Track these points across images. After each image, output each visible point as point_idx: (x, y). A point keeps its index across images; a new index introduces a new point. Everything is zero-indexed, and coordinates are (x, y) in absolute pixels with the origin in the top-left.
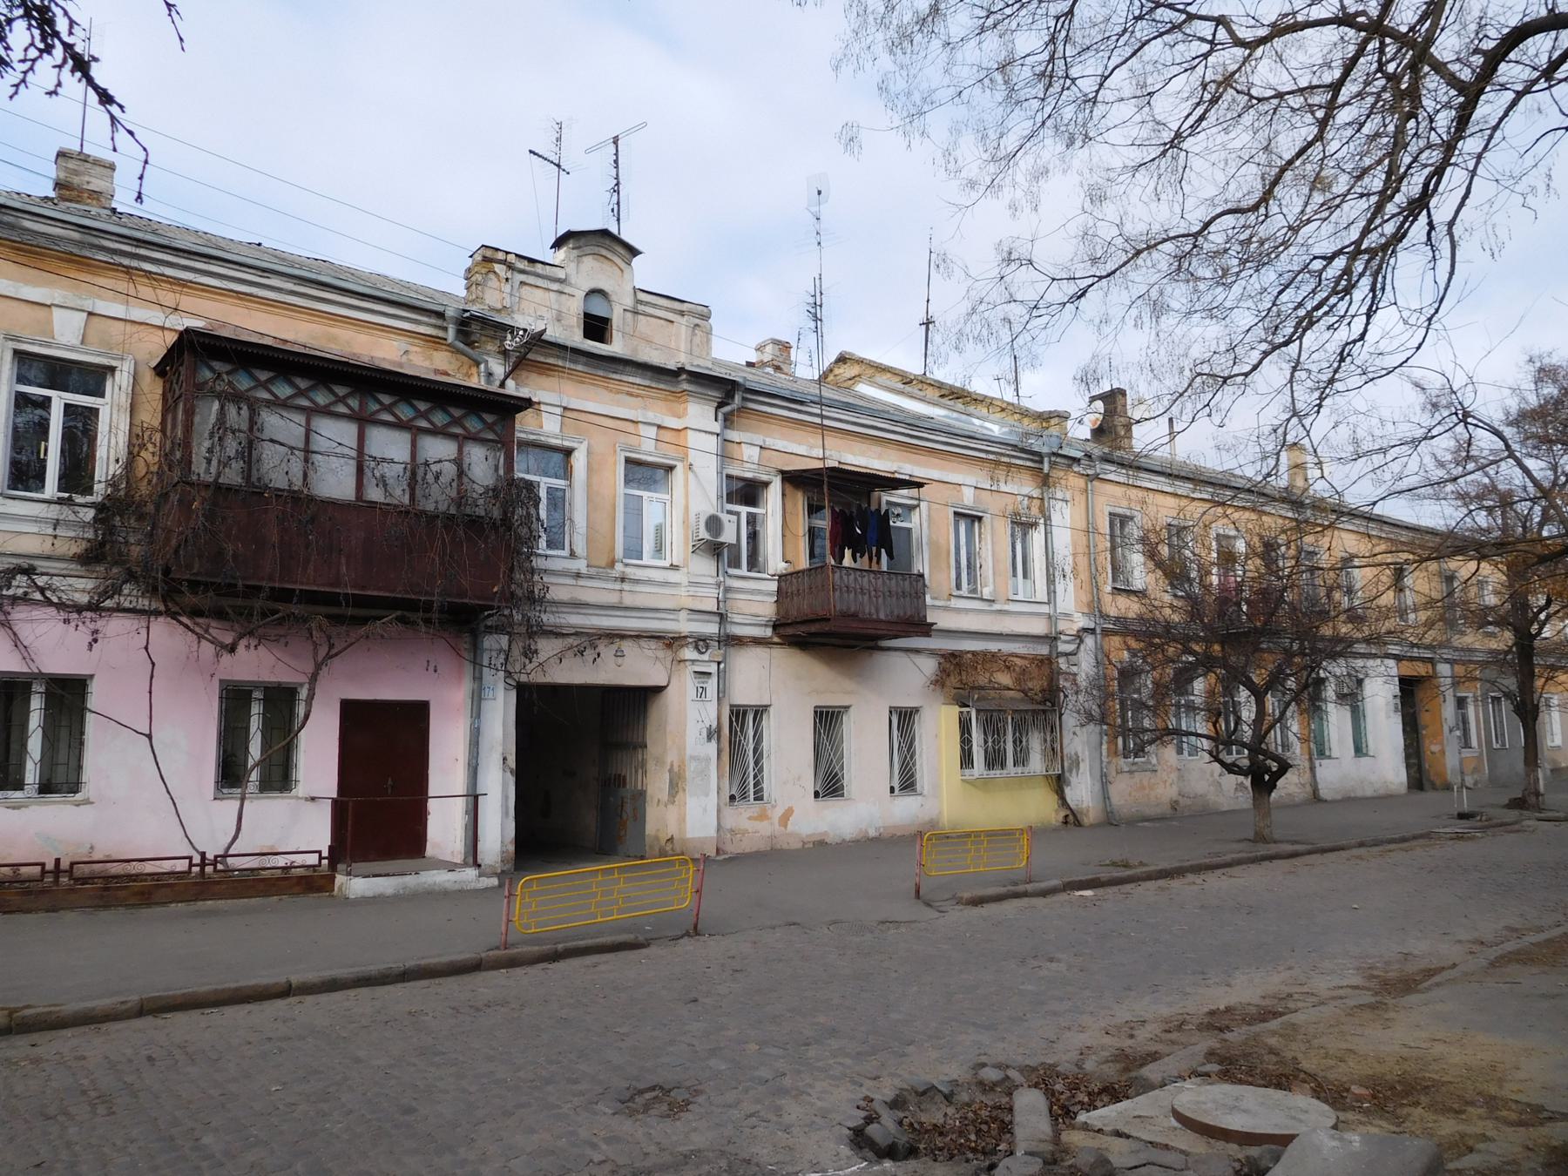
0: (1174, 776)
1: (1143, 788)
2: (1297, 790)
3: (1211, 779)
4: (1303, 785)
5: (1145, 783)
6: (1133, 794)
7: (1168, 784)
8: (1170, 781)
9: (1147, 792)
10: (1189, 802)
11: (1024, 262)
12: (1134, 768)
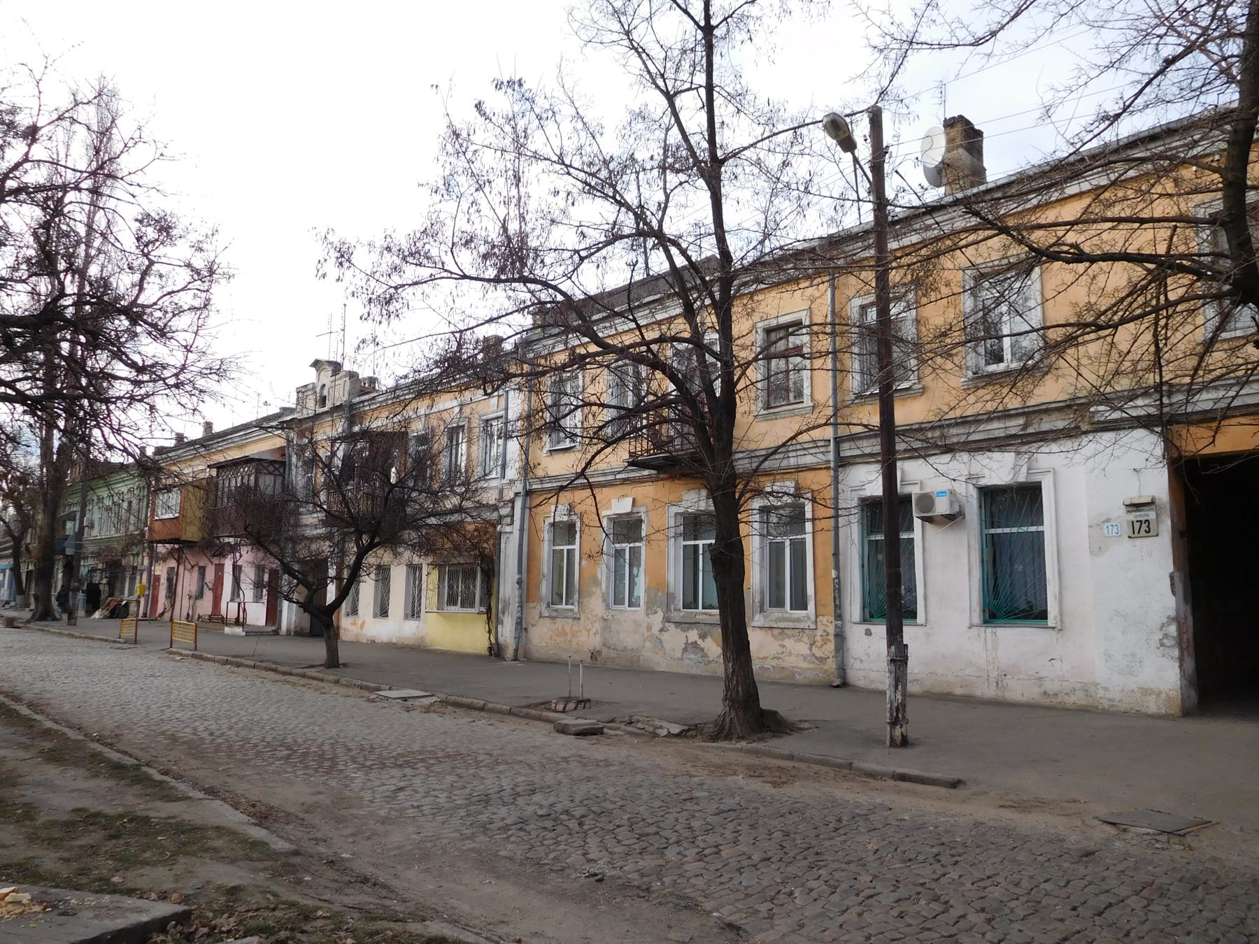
0: (598, 626)
1: (564, 634)
2: (805, 665)
3: (647, 634)
4: (822, 660)
5: (568, 629)
6: (554, 637)
7: (591, 633)
8: (594, 630)
9: (569, 638)
10: (613, 654)
11: (161, 549)
12: (554, 614)
